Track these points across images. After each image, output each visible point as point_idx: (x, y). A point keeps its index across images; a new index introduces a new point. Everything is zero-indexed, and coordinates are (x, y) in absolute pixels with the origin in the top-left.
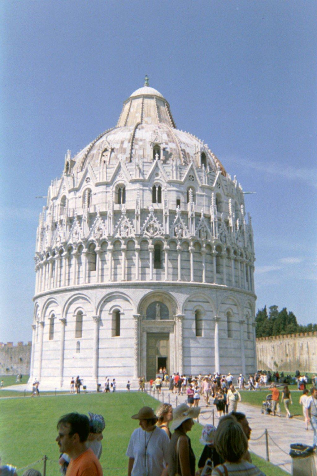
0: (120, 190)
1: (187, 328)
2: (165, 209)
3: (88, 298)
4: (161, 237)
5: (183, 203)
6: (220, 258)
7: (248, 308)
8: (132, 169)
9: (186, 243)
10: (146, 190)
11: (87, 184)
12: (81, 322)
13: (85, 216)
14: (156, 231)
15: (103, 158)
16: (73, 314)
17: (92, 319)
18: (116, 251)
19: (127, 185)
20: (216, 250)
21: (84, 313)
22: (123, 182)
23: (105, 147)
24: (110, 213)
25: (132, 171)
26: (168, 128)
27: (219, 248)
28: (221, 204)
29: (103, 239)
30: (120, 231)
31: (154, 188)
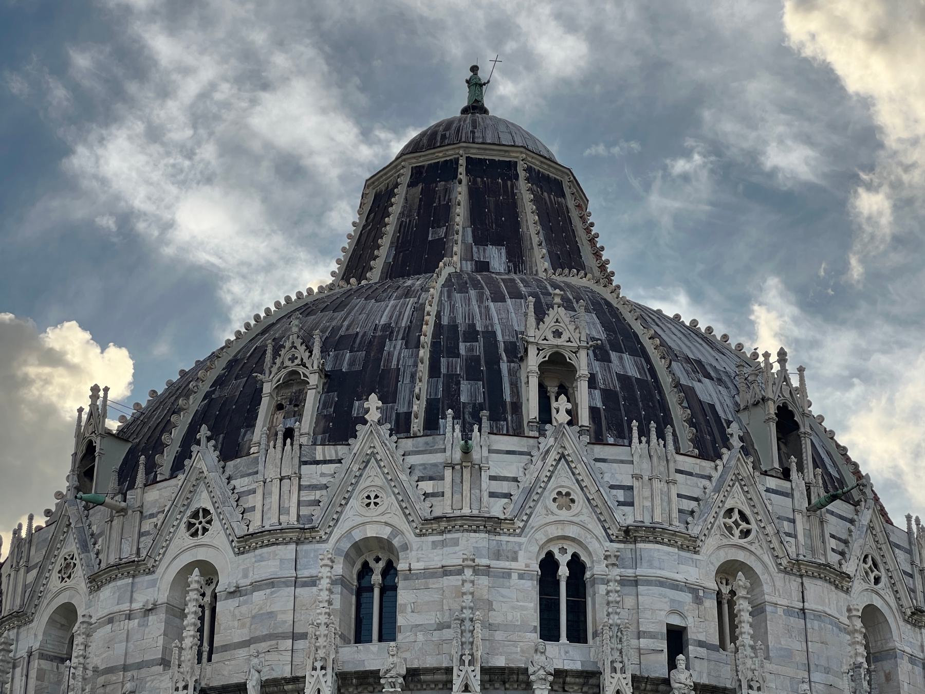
0: (366, 570)
5: (701, 644)
8: (435, 465)
10: (507, 574)
11: (192, 541)
19: (405, 547)
22: (385, 533)
23: (291, 366)
25: (431, 479)
28: (887, 665)
31: (549, 564)
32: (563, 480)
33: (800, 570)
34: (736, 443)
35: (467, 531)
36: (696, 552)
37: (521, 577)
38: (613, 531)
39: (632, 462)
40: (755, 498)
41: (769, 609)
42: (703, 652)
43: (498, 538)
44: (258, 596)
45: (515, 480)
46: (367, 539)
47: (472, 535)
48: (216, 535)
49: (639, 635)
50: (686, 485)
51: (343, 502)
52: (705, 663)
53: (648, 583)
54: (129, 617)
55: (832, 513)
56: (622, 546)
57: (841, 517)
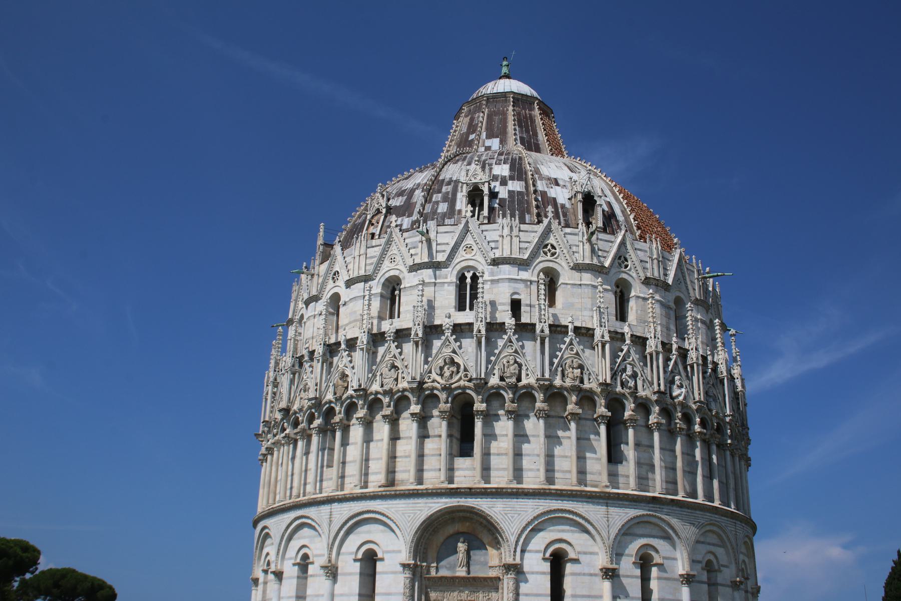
0: (394, 290)
1: (527, 595)
3: (317, 526)
4: (467, 384)
5: (527, 305)
6: (622, 426)
7: (714, 545)
9: (525, 395)
12: (306, 578)
13: (319, 350)
14: (458, 372)
16: (293, 561)
17: (322, 572)
19: (404, 278)
20: (608, 407)
21: (311, 560)
22: (396, 273)
24: (363, 339)
26: (521, 153)
27: (615, 403)
29: (347, 398)
31: (462, 278)
34: (550, 215)
46: (391, 277)
48: (341, 282)
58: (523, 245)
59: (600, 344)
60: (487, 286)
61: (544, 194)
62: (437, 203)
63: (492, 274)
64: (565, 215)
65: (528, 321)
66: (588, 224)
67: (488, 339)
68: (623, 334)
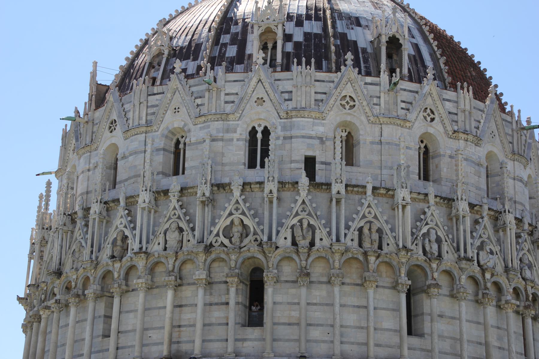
0: (178, 142)
2: (268, 181)
5: (322, 163)
6: (424, 296)
8: (202, 91)
14: (247, 236)
15: (153, 70)
18: (157, 287)
19: (189, 131)
24: (144, 198)
25: (200, 97)
28: (436, 160)
30: (166, 241)
31: (253, 132)
32: (260, 93)
33: (380, 121)
34: (349, 62)
35: (214, 121)
36: (323, 120)
37: (238, 140)
38: (283, 114)
39: (292, 79)
40: (358, 89)
41: (361, 142)
42: (323, 166)
43: (228, 122)
44: (131, 158)
45: (237, 94)
47: (216, 122)
49: (292, 162)
50: (319, 87)
51: (164, 112)
52: (324, 171)
53: (297, 137)
54: (89, 170)
55: (405, 90)
56: (286, 120)
57: (411, 91)
58: (319, 97)
59: (400, 207)
60: (280, 142)
61: (343, 37)
62: (225, 45)
63: (284, 128)
64: (366, 61)
65: (323, 180)
66: (392, 71)
67: (279, 199)
68: (426, 195)
